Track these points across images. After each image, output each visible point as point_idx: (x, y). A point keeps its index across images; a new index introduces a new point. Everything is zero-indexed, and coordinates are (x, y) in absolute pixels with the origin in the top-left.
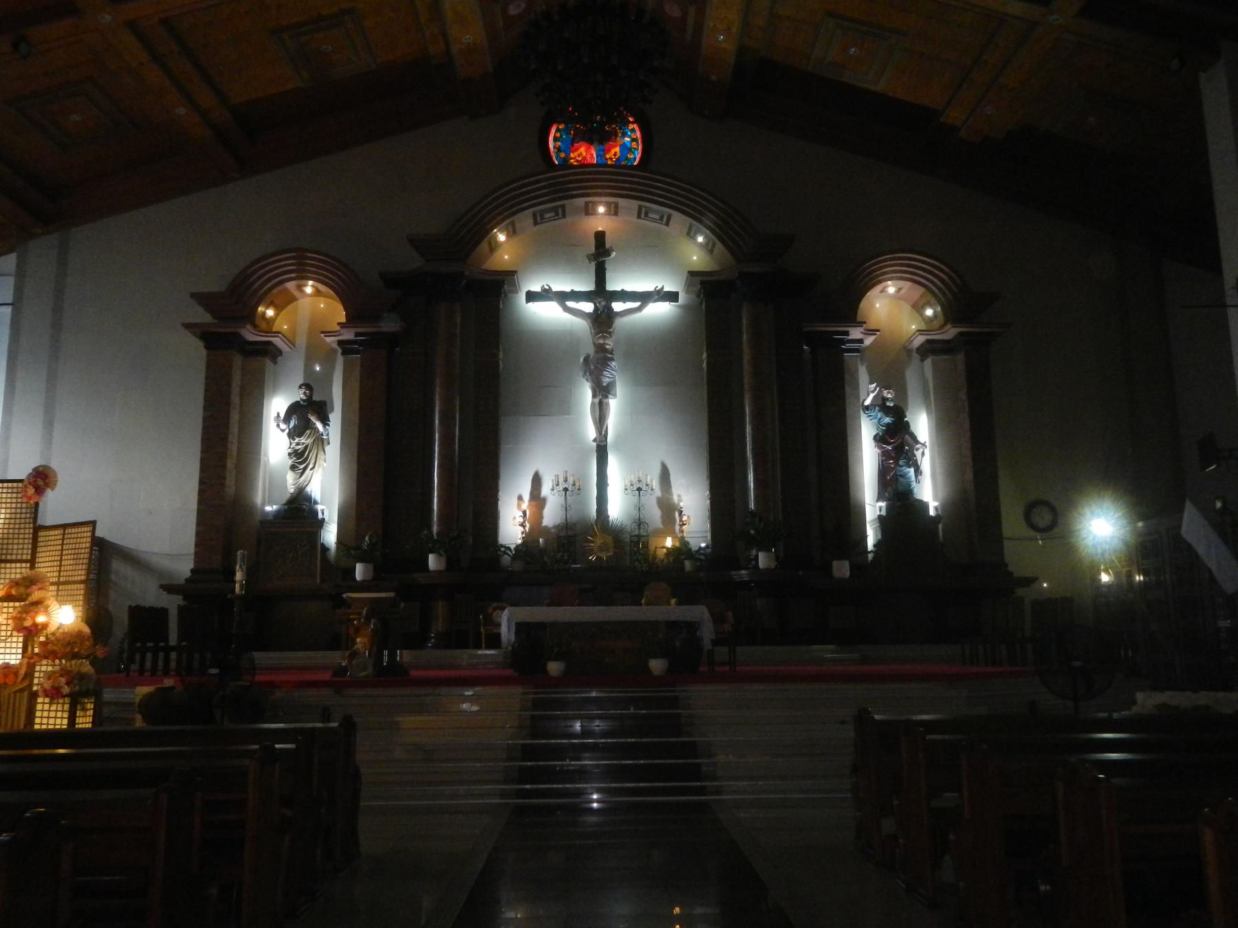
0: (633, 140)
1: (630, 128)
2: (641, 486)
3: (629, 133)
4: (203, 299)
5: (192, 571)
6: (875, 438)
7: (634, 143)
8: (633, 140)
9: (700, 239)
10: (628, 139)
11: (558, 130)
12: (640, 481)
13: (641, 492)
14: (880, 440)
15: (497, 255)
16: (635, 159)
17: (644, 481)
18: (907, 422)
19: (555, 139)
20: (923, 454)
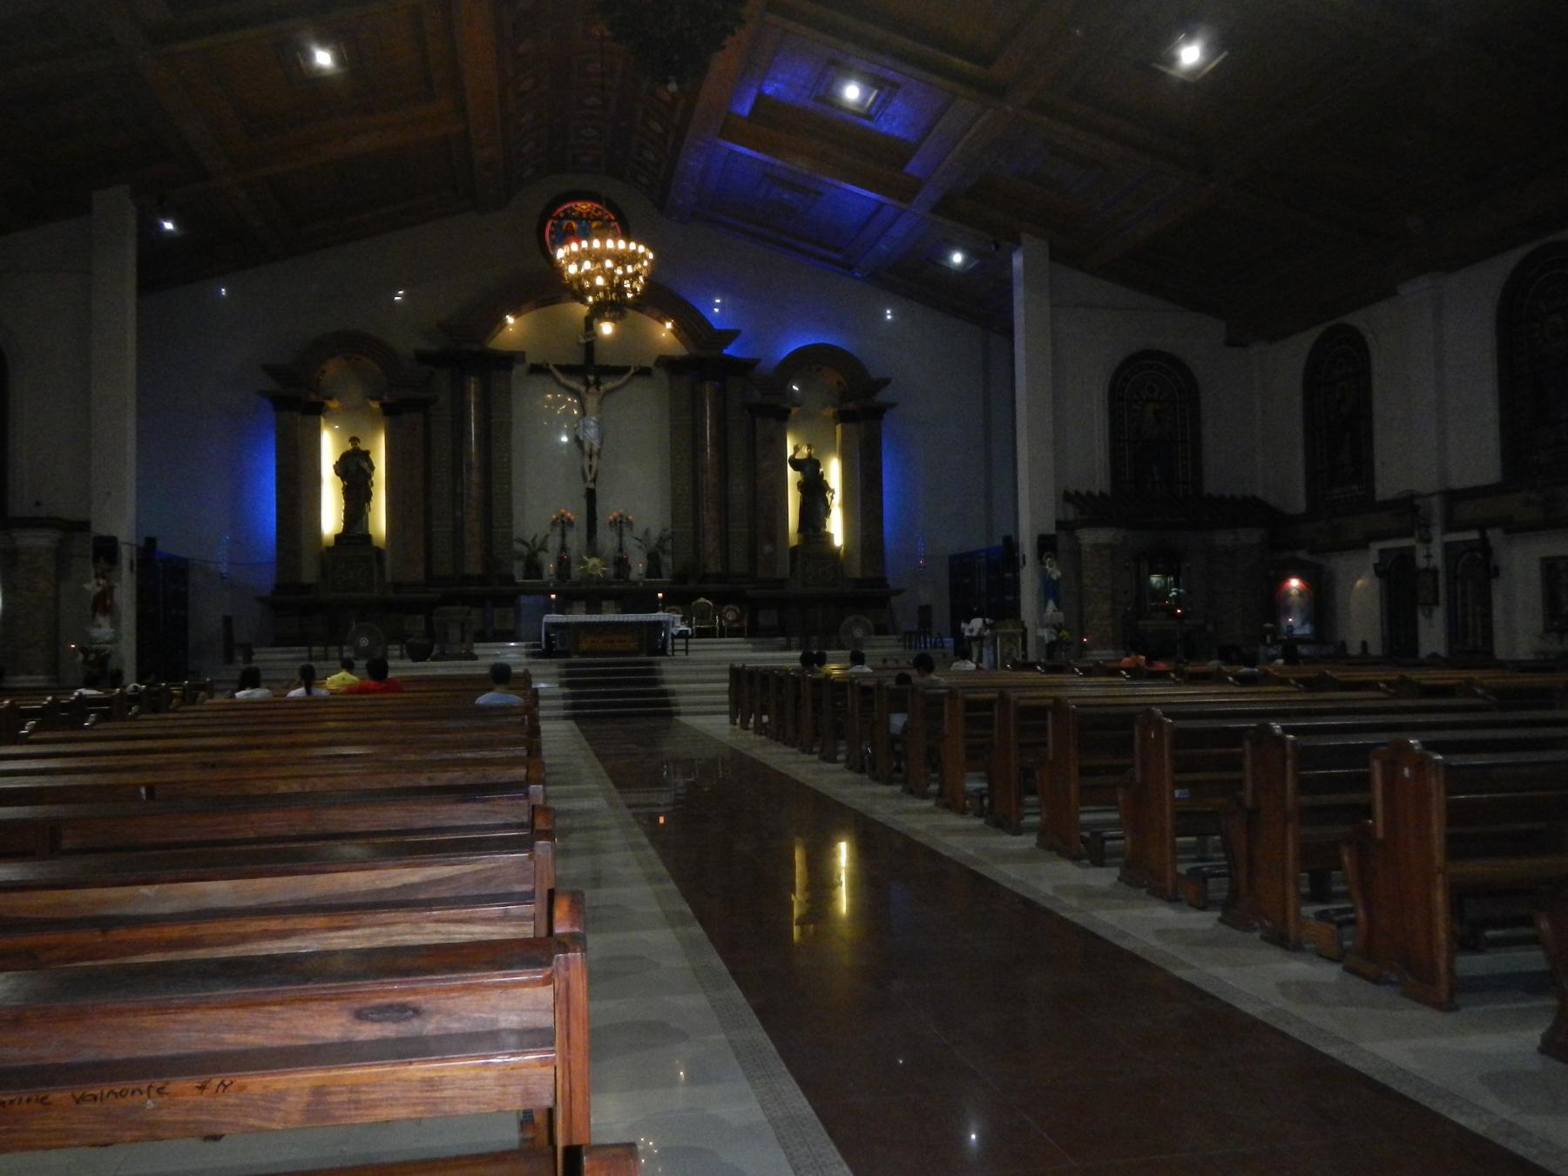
6: (798, 483)
9: (669, 325)
11: (553, 225)
14: (802, 486)
15: (505, 331)
19: (551, 233)
20: (832, 498)
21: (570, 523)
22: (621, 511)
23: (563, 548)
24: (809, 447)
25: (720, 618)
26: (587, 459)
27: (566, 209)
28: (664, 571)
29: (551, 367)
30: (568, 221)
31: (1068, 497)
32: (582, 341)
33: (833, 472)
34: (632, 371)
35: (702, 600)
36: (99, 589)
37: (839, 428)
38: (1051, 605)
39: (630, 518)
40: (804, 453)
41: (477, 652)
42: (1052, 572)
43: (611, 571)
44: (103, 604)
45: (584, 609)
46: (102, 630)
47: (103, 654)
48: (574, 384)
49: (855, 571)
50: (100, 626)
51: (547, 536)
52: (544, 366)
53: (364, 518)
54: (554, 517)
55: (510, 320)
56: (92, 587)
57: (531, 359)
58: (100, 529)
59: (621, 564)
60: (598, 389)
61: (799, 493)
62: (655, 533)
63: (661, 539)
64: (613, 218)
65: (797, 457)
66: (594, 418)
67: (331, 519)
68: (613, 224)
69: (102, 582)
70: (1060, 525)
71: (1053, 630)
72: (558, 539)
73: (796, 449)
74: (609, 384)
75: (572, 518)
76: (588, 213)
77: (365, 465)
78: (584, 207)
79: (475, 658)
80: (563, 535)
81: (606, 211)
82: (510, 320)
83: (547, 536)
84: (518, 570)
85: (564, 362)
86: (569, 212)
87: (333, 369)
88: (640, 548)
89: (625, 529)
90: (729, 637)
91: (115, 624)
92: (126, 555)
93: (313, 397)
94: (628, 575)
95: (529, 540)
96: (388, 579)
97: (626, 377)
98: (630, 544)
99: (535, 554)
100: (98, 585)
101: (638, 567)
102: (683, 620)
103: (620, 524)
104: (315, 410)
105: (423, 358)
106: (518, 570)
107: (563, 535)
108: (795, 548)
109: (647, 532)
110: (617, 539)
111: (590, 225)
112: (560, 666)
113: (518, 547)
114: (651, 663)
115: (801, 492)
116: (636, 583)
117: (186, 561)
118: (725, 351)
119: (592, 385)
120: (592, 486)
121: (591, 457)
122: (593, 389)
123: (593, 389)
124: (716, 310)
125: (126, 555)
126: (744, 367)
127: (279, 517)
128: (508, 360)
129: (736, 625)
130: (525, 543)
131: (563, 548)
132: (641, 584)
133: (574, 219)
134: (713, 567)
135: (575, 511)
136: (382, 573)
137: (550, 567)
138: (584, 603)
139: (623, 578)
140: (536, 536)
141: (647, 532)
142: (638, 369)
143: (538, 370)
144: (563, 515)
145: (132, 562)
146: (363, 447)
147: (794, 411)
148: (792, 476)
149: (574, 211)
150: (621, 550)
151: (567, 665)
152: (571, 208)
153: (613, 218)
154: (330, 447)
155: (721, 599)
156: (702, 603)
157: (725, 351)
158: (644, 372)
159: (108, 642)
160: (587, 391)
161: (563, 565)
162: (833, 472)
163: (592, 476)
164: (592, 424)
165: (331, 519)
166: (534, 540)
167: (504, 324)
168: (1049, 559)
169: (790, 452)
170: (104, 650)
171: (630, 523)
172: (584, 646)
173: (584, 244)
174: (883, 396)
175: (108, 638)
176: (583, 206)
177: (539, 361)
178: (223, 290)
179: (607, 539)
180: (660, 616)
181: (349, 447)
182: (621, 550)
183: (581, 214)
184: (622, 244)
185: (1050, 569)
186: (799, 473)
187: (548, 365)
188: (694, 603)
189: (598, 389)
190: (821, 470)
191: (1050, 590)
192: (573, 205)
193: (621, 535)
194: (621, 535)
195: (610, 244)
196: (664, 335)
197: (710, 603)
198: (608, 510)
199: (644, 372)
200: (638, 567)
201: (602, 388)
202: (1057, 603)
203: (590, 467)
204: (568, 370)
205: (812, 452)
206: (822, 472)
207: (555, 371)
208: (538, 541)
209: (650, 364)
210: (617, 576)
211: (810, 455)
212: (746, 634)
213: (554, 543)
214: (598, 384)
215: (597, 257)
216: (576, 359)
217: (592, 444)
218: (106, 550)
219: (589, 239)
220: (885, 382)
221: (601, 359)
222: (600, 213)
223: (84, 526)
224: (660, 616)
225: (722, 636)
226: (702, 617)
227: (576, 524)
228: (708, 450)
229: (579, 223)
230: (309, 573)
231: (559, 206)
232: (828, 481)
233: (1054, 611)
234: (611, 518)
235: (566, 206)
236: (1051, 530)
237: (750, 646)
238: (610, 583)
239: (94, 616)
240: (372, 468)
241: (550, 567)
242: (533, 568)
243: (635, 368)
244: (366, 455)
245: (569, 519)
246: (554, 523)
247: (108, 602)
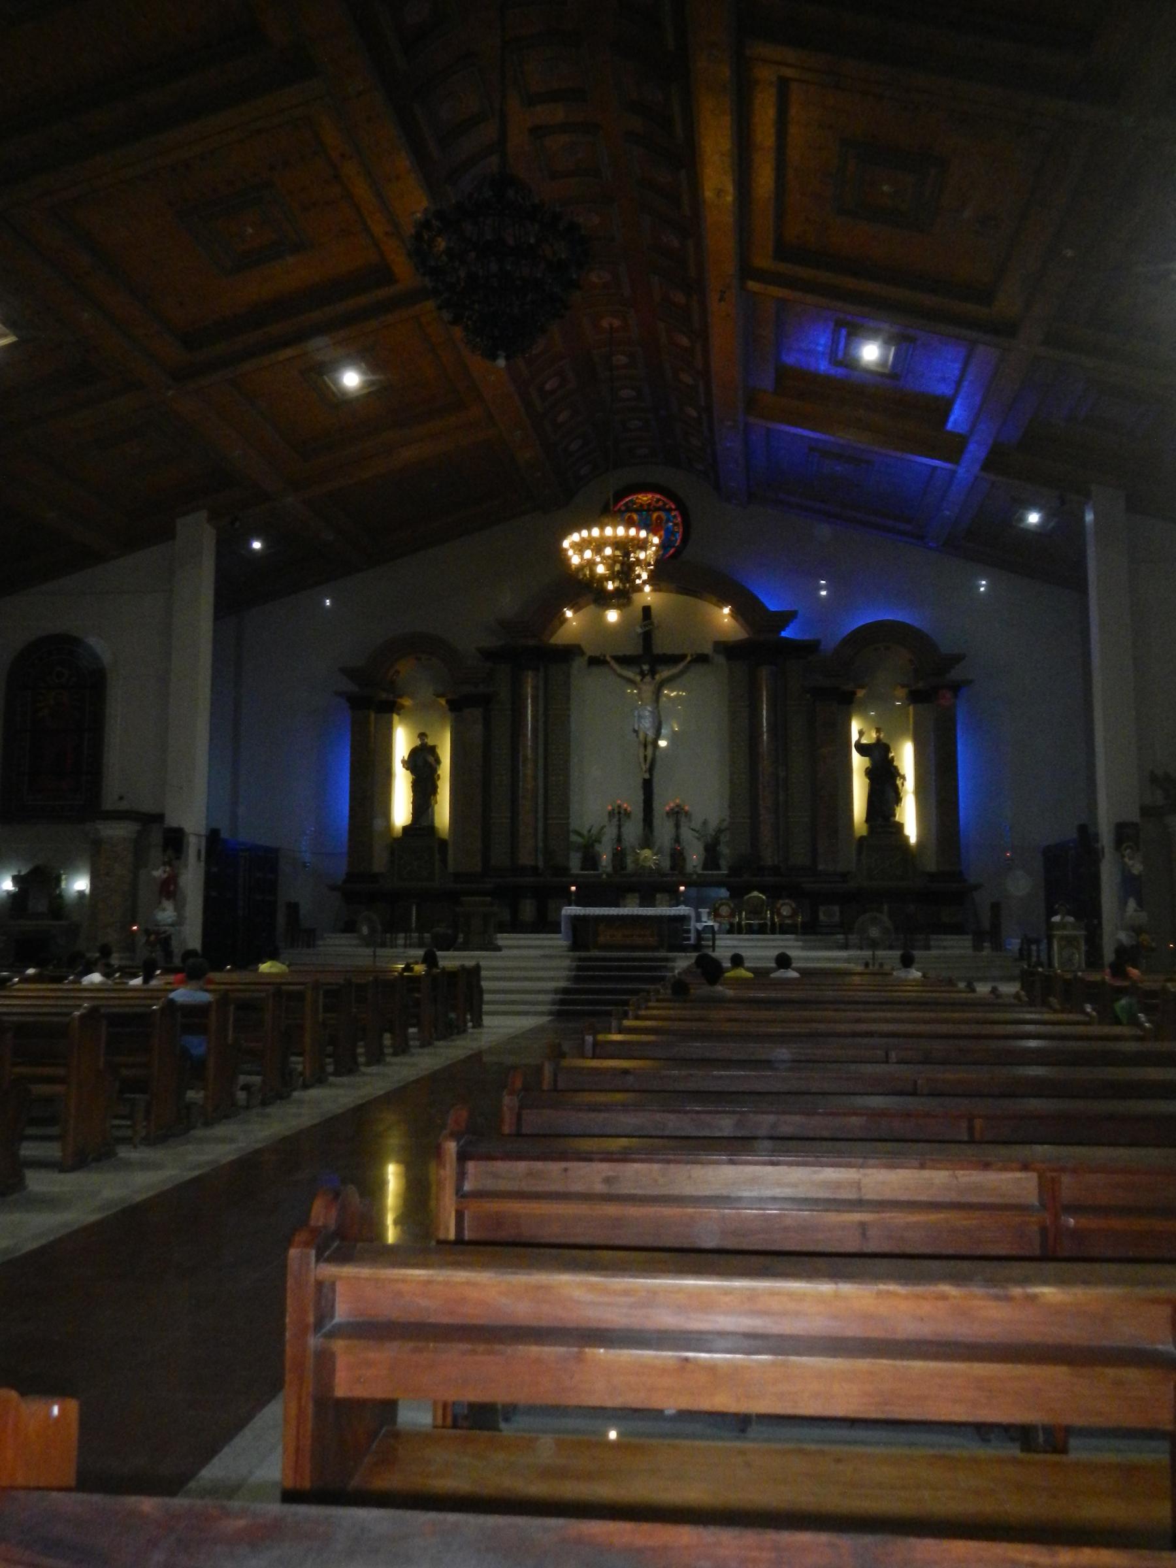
0: (676, 524)
1: (673, 514)
3: (672, 519)
4: (350, 673)
5: (347, 874)
6: (867, 769)
7: (676, 527)
8: (676, 524)
10: (671, 524)
14: (870, 773)
15: (565, 626)
16: (676, 540)
18: (893, 759)
20: (903, 785)
21: (628, 814)
22: (677, 801)
23: (619, 839)
24: (878, 730)
25: (772, 914)
26: (642, 749)
27: (627, 502)
28: (723, 863)
29: (608, 659)
30: (629, 514)
31: (1154, 779)
32: (639, 630)
33: (906, 757)
34: (689, 658)
35: (755, 893)
36: (165, 876)
37: (911, 708)
38: (1132, 904)
39: (687, 808)
40: (870, 738)
41: (500, 943)
42: (1133, 866)
43: (666, 864)
44: (169, 889)
45: (638, 901)
46: (166, 914)
47: (163, 936)
48: (630, 674)
49: (930, 864)
50: (164, 910)
51: (603, 828)
52: (602, 658)
53: (430, 810)
54: (610, 808)
55: (569, 614)
56: (159, 873)
57: (590, 651)
58: (172, 821)
59: (678, 857)
60: (653, 678)
61: (867, 781)
62: (713, 824)
63: (720, 831)
64: (673, 507)
65: (864, 741)
66: (649, 708)
67: (401, 812)
68: (674, 513)
69: (168, 869)
70: (1145, 811)
71: (1133, 934)
72: (614, 831)
73: (861, 733)
74: (665, 673)
75: (629, 809)
76: (649, 504)
77: (431, 759)
78: (645, 499)
79: (499, 949)
80: (619, 827)
81: (665, 500)
82: (569, 614)
83: (603, 828)
84: (575, 862)
85: (620, 654)
86: (630, 505)
87: (405, 669)
88: (698, 839)
89: (683, 819)
90: (780, 934)
91: (179, 908)
92: (194, 845)
93: (384, 696)
95: (585, 832)
96: (451, 869)
97: (681, 666)
98: (687, 834)
99: (592, 846)
100: (165, 872)
101: (695, 858)
102: (709, 914)
103: (677, 814)
104: (389, 708)
105: (488, 655)
106: (575, 862)
107: (619, 827)
108: (862, 838)
109: (705, 823)
110: (673, 830)
111: (651, 516)
112: (574, 959)
113: (574, 838)
114: (667, 959)
115: (869, 778)
117: (274, 851)
118: (783, 634)
119: (647, 675)
121: (645, 746)
122: (648, 679)
123: (648, 679)
124: (824, 593)
125: (194, 845)
126: (806, 649)
127: (352, 809)
128: (569, 652)
129: (788, 921)
130: (579, 834)
131: (619, 839)
133: (636, 511)
134: (769, 857)
135: (632, 802)
136: (444, 861)
137: (605, 858)
138: (637, 895)
140: (592, 826)
142: (694, 657)
143: (596, 661)
144: (619, 807)
145: (199, 851)
146: (430, 742)
147: (861, 693)
148: (858, 762)
149: (635, 504)
151: (580, 959)
152: (631, 501)
153: (673, 507)
154: (402, 742)
155: (775, 893)
156: (754, 897)
157: (783, 634)
158: (702, 659)
159: (172, 925)
160: (642, 680)
161: (619, 856)
162: (906, 757)
163: (648, 766)
164: (647, 714)
165: (401, 812)
167: (565, 620)
168: (1128, 851)
169: (855, 737)
170: (165, 932)
171: (687, 814)
172: (602, 939)
173: (585, 533)
174: (955, 674)
175: (170, 921)
176: (644, 498)
178: (328, 604)
179: (664, 831)
180: (682, 910)
181: (418, 742)
183: (642, 505)
184: (621, 531)
185: (1130, 863)
186: (867, 759)
187: (605, 656)
188: (747, 897)
189: (653, 678)
190: (891, 755)
191: (1130, 885)
192: (633, 497)
193: (677, 826)
194: (677, 826)
195: (609, 531)
196: (726, 620)
197: (764, 897)
198: (664, 803)
199: (702, 659)
200: (695, 858)
201: (657, 677)
202: (1140, 903)
203: (645, 757)
204: (625, 660)
205: (882, 736)
206: (893, 757)
207: (613, 663)
208: (594, 831)
209: (708, 649)
210: (672, 868)
211: (878, 739)
212: (768, 931)
213: (610, 833)
214: (653, 673)
215: (598, 546)
216: (632, 648)
217: (646, 735)
218: (175, 840)
219: (589, 528)
220: (958, 659)
221: (662, 645)
222: (661, 504)
223: (159, 818)
224: (682, 910)
225: (773, 932)
226: (756, 911)
228: (765, 737)
229: (641, 515)
230: (380, 862)
231: (622, 500)
232: (899, 767)
233: (1136, 911)
234: (668, 808)
235: (627, 500)
236: (1134, 816)
237: (800, 944)
238: (665, 875)
239: (160, 903)
240: (438, 761)
241: (605, 858)
242: (590, 860)
243: (692, 655)
244: (432, 750)
245: (625, 810)
246: (611, 814)
247: (172, 888)
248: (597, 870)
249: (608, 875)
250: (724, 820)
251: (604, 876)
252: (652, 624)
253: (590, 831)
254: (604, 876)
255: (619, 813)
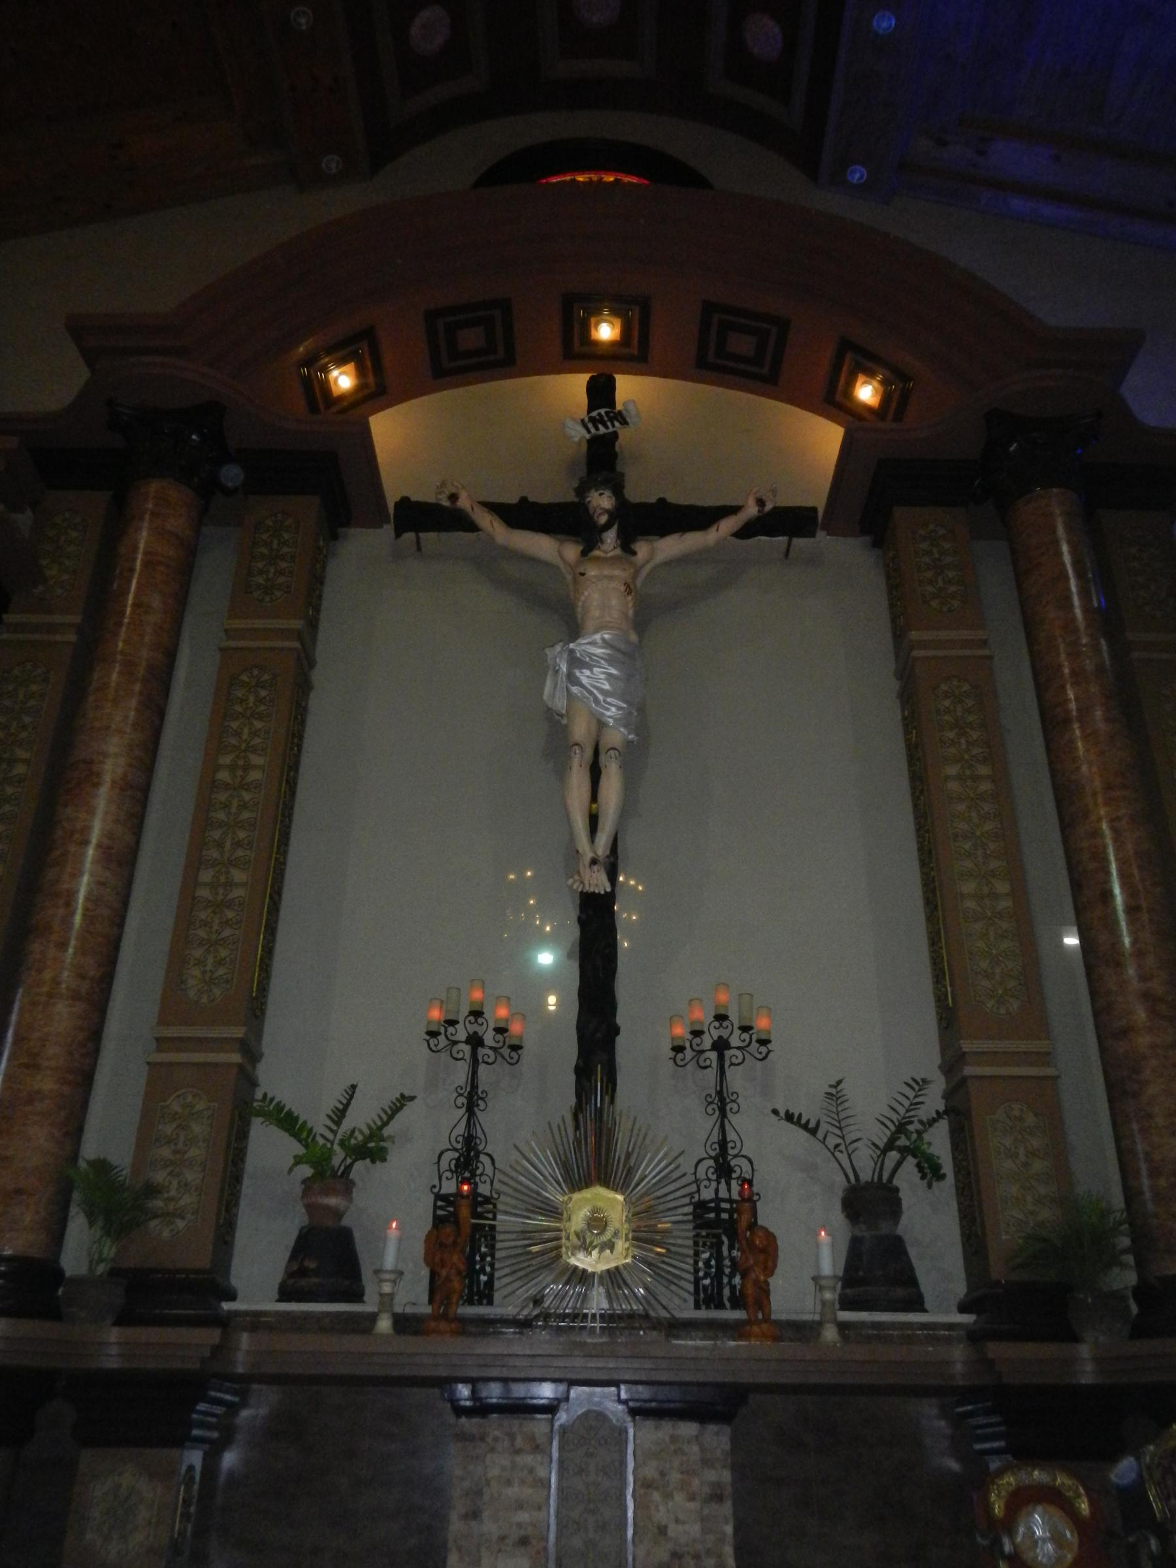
2: (725, 1034)
12: (721, 1018)
13: (728, 1053)
17: (734, 1017)
22: (723, 997)
29: (464, 503)
34: (752, 510)
48: (541, 545)
52: (446, 503)
54: (436, 1014)
80: (473, 1099)
83: (404, 1100)
85: (512, 498)
94: (764, 1291)
95: (319, 1123)
107: (473, 1099)
109: (835, 1095)
110: (705, 1126)
116: (803, 1331)
120: (598, 882)
132: (830, 1334)
139: (737, 1302)
141: (835, 1095)
142: (769, 507)
150: (724, 1170)
160: (584, 553)
166: (339, 1115)
177: (423, 494)
182: (724, 1170)
187: (453, 497)
207: (486, 520)
208: (360, 1118)
214: (626, 545)
217: (601, 725)
227: (528, 1054)
238: (675, 1327)
243: (761, 502)
248: (356, 1296)
249: (405, 1324)
250: (920, 1085)
251: (384, 1324)
252: (621, 418)
253: (339, 1115)
254: (384, 1324)
255: (475, 1041)
